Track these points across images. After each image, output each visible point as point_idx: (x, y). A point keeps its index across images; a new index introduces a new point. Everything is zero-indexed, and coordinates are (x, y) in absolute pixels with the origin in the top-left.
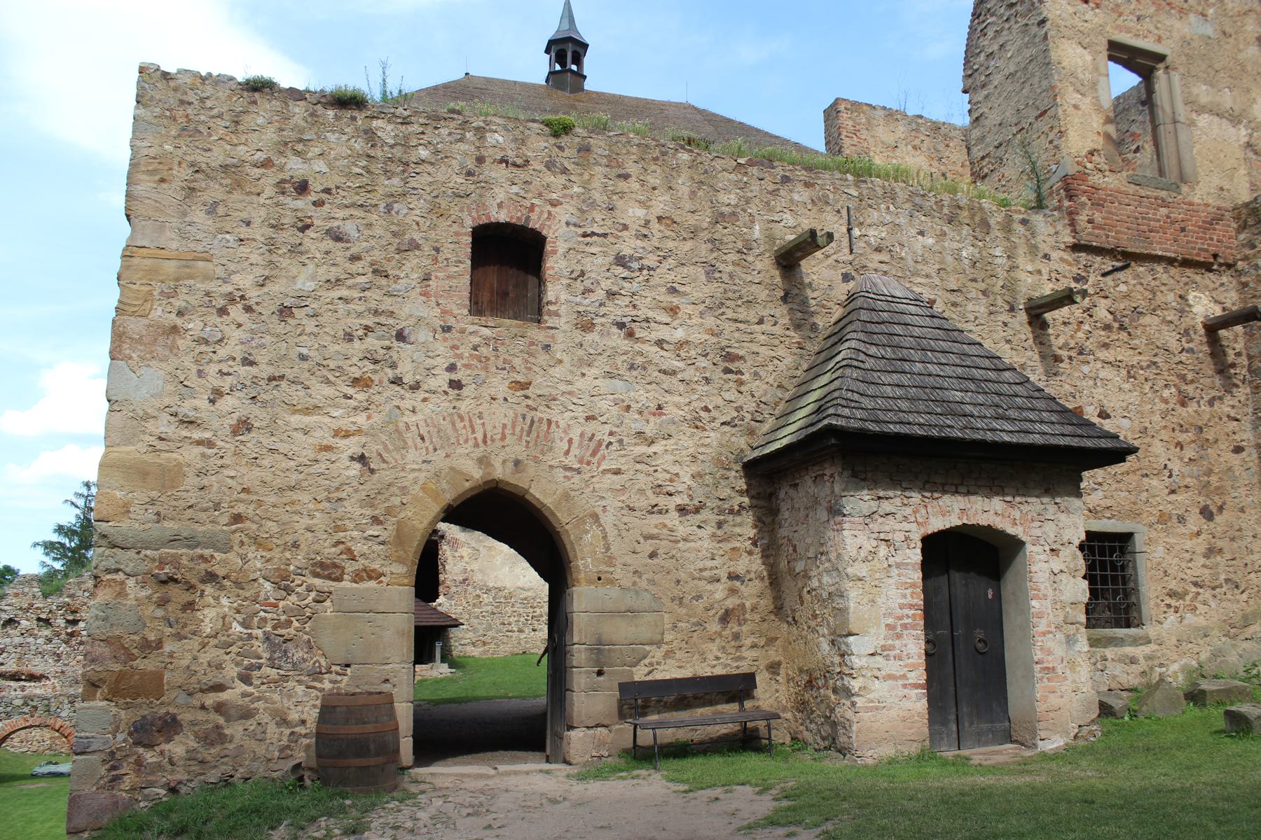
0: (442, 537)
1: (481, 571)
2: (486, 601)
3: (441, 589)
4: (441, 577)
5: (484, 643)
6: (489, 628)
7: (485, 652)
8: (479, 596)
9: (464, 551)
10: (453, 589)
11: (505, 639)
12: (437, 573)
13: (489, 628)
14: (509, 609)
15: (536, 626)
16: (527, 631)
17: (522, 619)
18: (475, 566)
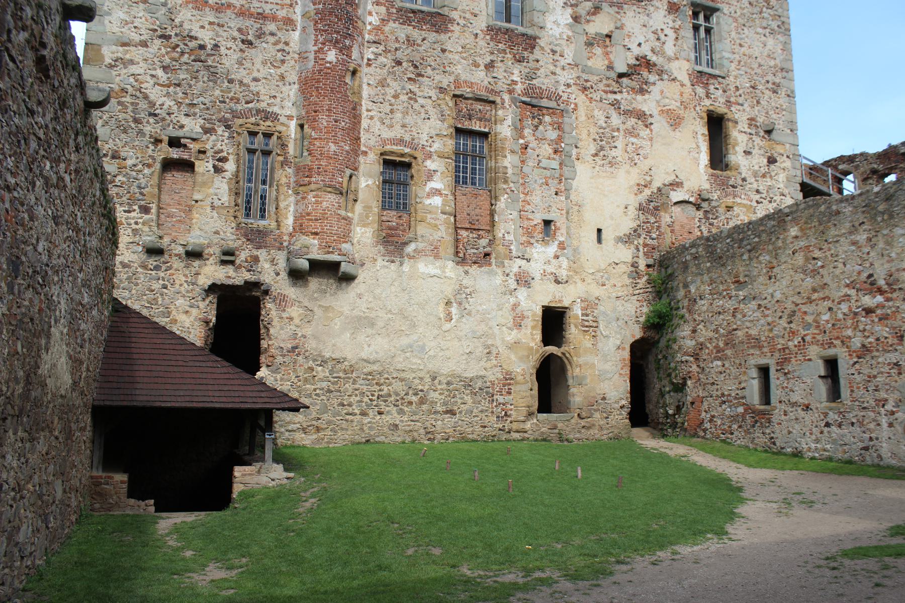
0: (266, 292)
1: (315, 337)
2: (321, 375)
3: (263, 359)
4: (264, 344)
5: (318, 429)
6: (325, 410)
7: (318, 440)
8: (312, 369)
9: (294, 312)
10: (279, 359)
11: (344, 424)
12: (257, 338)
13: (325, 410)
14: (349, 386)
15: (383, 408)
16: (371, 413)
17: (366, 399)
18: (308, 330)
